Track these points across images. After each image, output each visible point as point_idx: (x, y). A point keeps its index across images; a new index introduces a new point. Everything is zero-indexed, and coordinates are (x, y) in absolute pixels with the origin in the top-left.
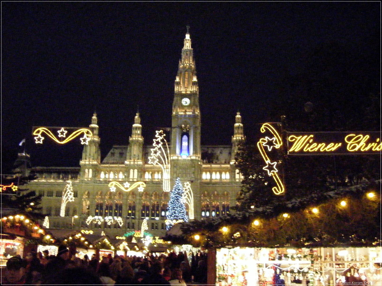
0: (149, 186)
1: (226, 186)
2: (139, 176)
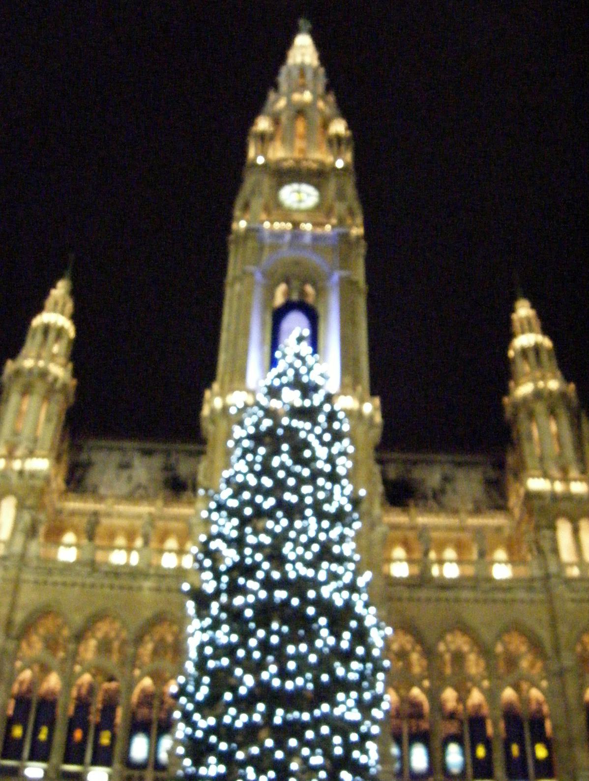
0: (74, 585)
1: (513, 601)
2: (21, 526)
